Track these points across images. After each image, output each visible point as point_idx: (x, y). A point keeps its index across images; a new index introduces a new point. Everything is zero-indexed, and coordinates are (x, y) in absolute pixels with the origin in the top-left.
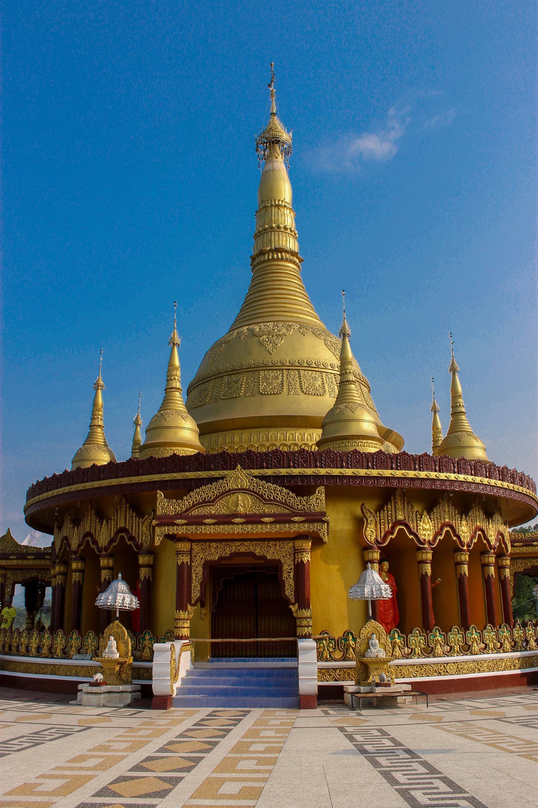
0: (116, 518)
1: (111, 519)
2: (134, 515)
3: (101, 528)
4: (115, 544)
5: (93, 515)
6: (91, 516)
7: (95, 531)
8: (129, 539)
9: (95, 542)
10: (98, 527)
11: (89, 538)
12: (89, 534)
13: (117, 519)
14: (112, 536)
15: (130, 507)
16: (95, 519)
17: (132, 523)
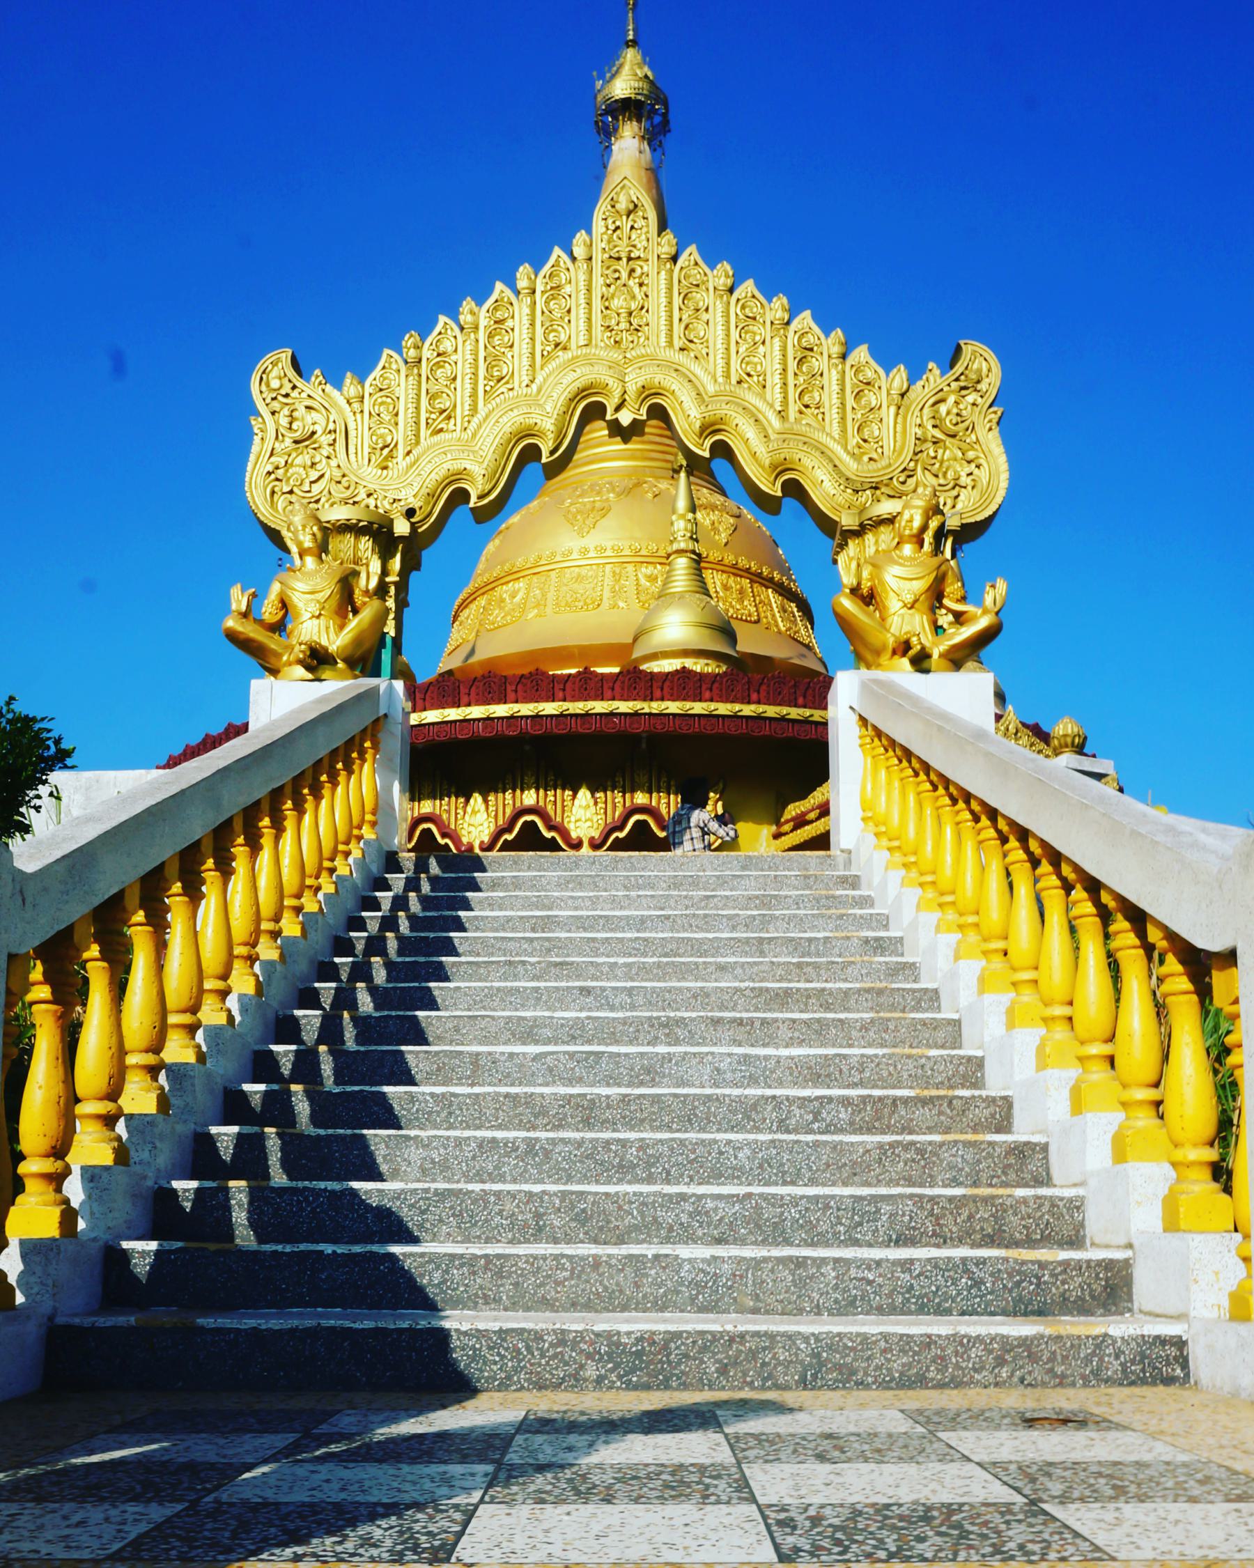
8: (444, 835)
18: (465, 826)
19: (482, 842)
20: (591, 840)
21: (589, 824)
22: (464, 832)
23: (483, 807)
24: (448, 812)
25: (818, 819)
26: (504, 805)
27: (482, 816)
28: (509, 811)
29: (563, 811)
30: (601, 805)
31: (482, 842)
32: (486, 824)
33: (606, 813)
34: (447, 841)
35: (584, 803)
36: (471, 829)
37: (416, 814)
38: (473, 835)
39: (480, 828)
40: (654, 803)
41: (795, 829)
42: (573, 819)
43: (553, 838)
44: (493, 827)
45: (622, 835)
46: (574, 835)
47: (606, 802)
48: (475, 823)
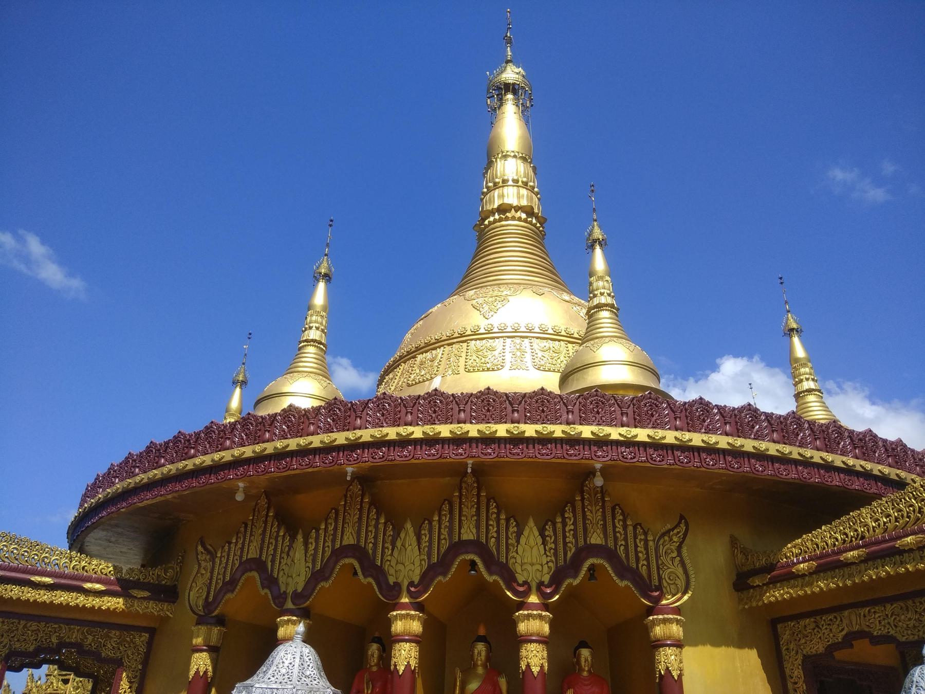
0: (331, 528)
1: (317, 531)
2: (382, 521)
3: (290, 547)
5: (270, 520)
6: (266, 522)
7: (274, 556)
11: (255, 574)
12: (258, 564)
13: (335, 529)
14: (318, 567)
15: (371, 504)
16: (275, 529)
17: (376, 538)
18: (393, 563)
19: (411, 584)
22: (392, 571)
23: (415, 543)
24: (375, 545)
28: (445, 545)
32: (417, 563)
36: (400, 567)
40: (611, 544)
42: (519, 560)
43: (494, 580)
44: (425, 567)
45: (576, 582)
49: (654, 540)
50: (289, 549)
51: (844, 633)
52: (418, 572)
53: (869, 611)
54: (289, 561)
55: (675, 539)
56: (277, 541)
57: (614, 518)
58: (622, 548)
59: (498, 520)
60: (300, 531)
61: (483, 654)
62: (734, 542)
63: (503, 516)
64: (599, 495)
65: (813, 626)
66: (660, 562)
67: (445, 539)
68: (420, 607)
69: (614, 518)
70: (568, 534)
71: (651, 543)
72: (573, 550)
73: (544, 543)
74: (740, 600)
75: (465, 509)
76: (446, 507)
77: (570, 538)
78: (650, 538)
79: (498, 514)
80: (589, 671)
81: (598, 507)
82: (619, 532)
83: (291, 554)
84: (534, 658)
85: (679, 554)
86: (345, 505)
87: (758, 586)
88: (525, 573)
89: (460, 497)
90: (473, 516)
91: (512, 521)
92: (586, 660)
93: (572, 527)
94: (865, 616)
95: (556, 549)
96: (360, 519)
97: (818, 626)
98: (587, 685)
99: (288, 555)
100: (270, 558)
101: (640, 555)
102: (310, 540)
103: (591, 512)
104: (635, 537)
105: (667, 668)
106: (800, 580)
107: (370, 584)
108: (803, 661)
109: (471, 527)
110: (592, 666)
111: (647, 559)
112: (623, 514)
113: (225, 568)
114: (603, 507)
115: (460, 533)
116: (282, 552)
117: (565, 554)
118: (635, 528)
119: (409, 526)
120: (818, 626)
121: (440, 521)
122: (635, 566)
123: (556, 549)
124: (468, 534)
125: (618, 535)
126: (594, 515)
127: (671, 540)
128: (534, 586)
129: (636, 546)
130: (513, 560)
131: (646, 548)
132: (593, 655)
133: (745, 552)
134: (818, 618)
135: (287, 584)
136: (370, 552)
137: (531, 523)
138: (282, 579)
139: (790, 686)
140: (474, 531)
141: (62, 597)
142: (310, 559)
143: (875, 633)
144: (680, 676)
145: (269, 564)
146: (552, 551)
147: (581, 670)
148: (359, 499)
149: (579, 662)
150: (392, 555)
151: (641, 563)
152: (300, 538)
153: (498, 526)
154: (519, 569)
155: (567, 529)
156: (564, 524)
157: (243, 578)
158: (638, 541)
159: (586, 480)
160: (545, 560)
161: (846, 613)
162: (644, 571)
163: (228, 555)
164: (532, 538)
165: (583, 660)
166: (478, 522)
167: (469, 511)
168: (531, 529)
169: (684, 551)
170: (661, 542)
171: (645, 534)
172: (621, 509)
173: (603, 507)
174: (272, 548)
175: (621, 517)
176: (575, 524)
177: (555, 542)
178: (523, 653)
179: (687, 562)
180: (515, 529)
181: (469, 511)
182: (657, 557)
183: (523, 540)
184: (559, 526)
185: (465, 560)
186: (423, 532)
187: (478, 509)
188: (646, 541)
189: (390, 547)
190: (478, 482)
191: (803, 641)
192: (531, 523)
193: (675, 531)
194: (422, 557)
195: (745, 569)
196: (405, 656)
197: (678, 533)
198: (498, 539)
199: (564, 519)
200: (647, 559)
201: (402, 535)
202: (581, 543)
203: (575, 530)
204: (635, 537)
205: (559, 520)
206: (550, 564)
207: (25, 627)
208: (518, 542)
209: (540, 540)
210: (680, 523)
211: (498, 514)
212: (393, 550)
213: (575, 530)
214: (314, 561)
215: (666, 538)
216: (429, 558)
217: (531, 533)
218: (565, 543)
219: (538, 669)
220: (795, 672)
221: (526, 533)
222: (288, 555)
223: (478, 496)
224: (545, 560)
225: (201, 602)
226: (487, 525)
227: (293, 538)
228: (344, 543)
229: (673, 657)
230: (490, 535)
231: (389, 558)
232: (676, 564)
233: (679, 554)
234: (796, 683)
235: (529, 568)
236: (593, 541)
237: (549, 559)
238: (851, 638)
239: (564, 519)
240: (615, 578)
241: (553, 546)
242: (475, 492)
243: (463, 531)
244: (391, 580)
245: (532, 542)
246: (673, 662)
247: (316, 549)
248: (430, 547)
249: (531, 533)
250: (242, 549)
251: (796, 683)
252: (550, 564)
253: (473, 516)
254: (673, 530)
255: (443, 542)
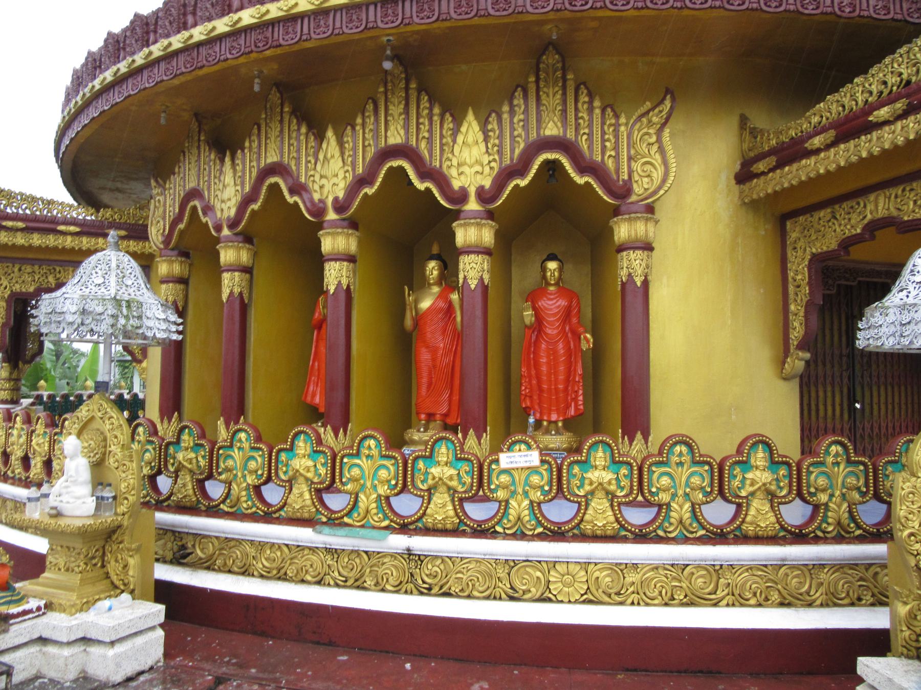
3: (221, 171)
4: (255, 206)
7: (209, 181)
8: (292, 192)
9: (208, 209)
10: (215, 168)
11: (197, 203)
12: (194, 194)
14: (247, 189)
15: (293, 113)
17: (298, 151)
18: (317, 178)
19: (336, 199)
20: (480, 192)
21: (478, 168)
22: (316, 187)
23: (337, 153)
24: (298, 159)
25: (828, 147)
26: (364, 147)
27: (336, 164)
28: (371, 152)
29: (442, 151)
30: (494, 141)
31: (336, 199)
32: (341, 175)
33: (500, 153)
34: (296, 198)
35: (470, 139)
36: (324, 181)
37: (262, 165)
38: (326, 190)
39: (335, 180)
40: (571, 135)
41: (780, 165)
42: (455, 162)
43: (428, 189)
44: (350, 177)
45: (523, 183)
46: (456, 184)
47: (500, 137)
48: (329, 174)
49: (626, 124)
50: (220, 174)
51: (866, 221)
52: (342, 185)
53: (904, 190)
54: (221, 187)
55: (655, 119)
56: (210, 166)
57: (576, 101)
58: (585, 137)
59: (430, 117)
60: (228, 153)
61: (435, 273)
62: (743, 121)
63: (436, 110)
64: (559, 74)
65: (829, 216)
66: (632, 152)
67: (369, 145)
68: (353, 224)
69: (576, 101)
70: (516, 126)
71: (622, 128)
72: (522, 146)
73: (486, 139)
74: (741, 192)
75: (391, 107)
76: (370, 107)
77: (519, 131)
78: (623, 120)
79: (431, 109)
80: (557, 284)
81: (557, 89)
82: (582, 118)
83: (222, 178)
84: (473, 270)
85: (659, 140)
86: (266, 118)
87: (763, 173)
88: (462, 177)
89: (386, 93)
90: (400, 114)
91: (448, 115)
92: (553, 274)
93: (522, 117)
94: (896, 197)
95: (500, 146)
96: (281, 131)
97: (835, 218)
98: (552, 299)
99: (220, 180)
100: (205, 188)
101: (608, 144)
102: (237, 162)
103: (548, 96)
104: (603, 123)
105: (630, 275)
106: (813, 159)
107: (296, 203)
108: (810, 261)
109: (399, 127)
110: (560, 278)
111: (616, 148)
112: (591, 95)
113: (174, 199)
114: (564, 88)
115: (386, 137)
116: (215, 177)
117: (512, 151)
118: (603, 111)
119: (330, 134)
120: (835, 218)
121: (363, 125)
122: (599, 159)
123: (500, 146)
124: (395, 137)
125: (581, 121)
126: (552, 99)
127: (650, 121)
128: (472, 191)
129: (603, 133)
130: (449, 163)
131: (617, 137)
132: (561, 269)
133: (754, 133)
134: (837, 207)
135: (222, 210)
136: (294, 168)
137: (470, 117)
138: (218, 206)
139: (791, 289)
140: (402, 132)
141: (37, 240)
142: (238, 182)
143: (906, 218)
144: (646, 283)
145: (206, 193)
146: (496, 149)
147: (548, 284)
148: (278, 110)
149: (544, 277)
150: (315, 169)
151: (608, 154)
152: (227, 159)
153: (431, 124)
154: (454, 172)
155: (515, 120)
156: (512, 113)
157: (188, 209)
158: (606, 128)
159: (544, 53)
160: (486, 159)
161: (872, 197)
162: (610, 164)
163: (175, 186)
164: (471, 132)
165: (549, 274)
166: (407, 119)
167: (396, 109)
168: (470, 124)
169: (667, 132)
170: (637, 127)
171: (617, 117)
172: (587, 88)
173: (564, 88)
174: (206, 173)
175: (587, 99)
176: (526, 112)
177: (500, 137)
178: (461, 266)
179: (669, 148)
180: (451, 126)
181: (396, 109)
182: (628, 145)
183: (460, 139)
184: (505, 116)
185: (391, 168)
186: (345, 139)
187: (407, 105)
188: (617, 126)
189: (313, 161)
190: (406, 72)
191: (813, 237)
192: (470, 117)
193: (656, 111)
194: (346, 168)
195: (752, 154)
196: (335, 275)
197: (661, 112)
198: (430, 140)
199: (512, 106)
200: (616, 148)
201: (324, 146)
202: (533, 136)
203: (526, 121)
204: (603, 123)
205: (506, 108)
206: (493, 164)
207: (20, 270)
208: (454, 141)
209: (480, 137)
210: (664, 99)
211: (431, 109)
212: (316, 164)
213: (526, 121)
214: (243, 184)
215: (644, 120)
216: (354, 170)
217: (471, 128)
218: (513, 138)
219: (476, 282)
220: (799, 271)
221: (463, 129)
222: (220, 180)
223: (407, 89)
224: (486, 159)
225: (160, 238)
226: (418, 124)
227: (222, 161)
228: (269, 161)
229: (637, 262)
230: (421, 136)
231: (312, 173)
232: (652, 153)
233: (659, 140)
234: (798, 286)
235: (466, 169)
236: (548, 132)
237: (491, 158)
238: (874, 227)
239: (512, 106)
240: (573, 175)
241: (497, 141)
242: (402, 85)
243: (389, 134)
244: (316, 197)
245: (470, 139)
246: (637, 268)
247: (243, 170)
248: (354, 156)
249: (471, 128)
250: (184, 178)
251: (798, 286)
252: (493, 164)
253: (400, 114)
254: (653, 109)
255: (368, 149)
